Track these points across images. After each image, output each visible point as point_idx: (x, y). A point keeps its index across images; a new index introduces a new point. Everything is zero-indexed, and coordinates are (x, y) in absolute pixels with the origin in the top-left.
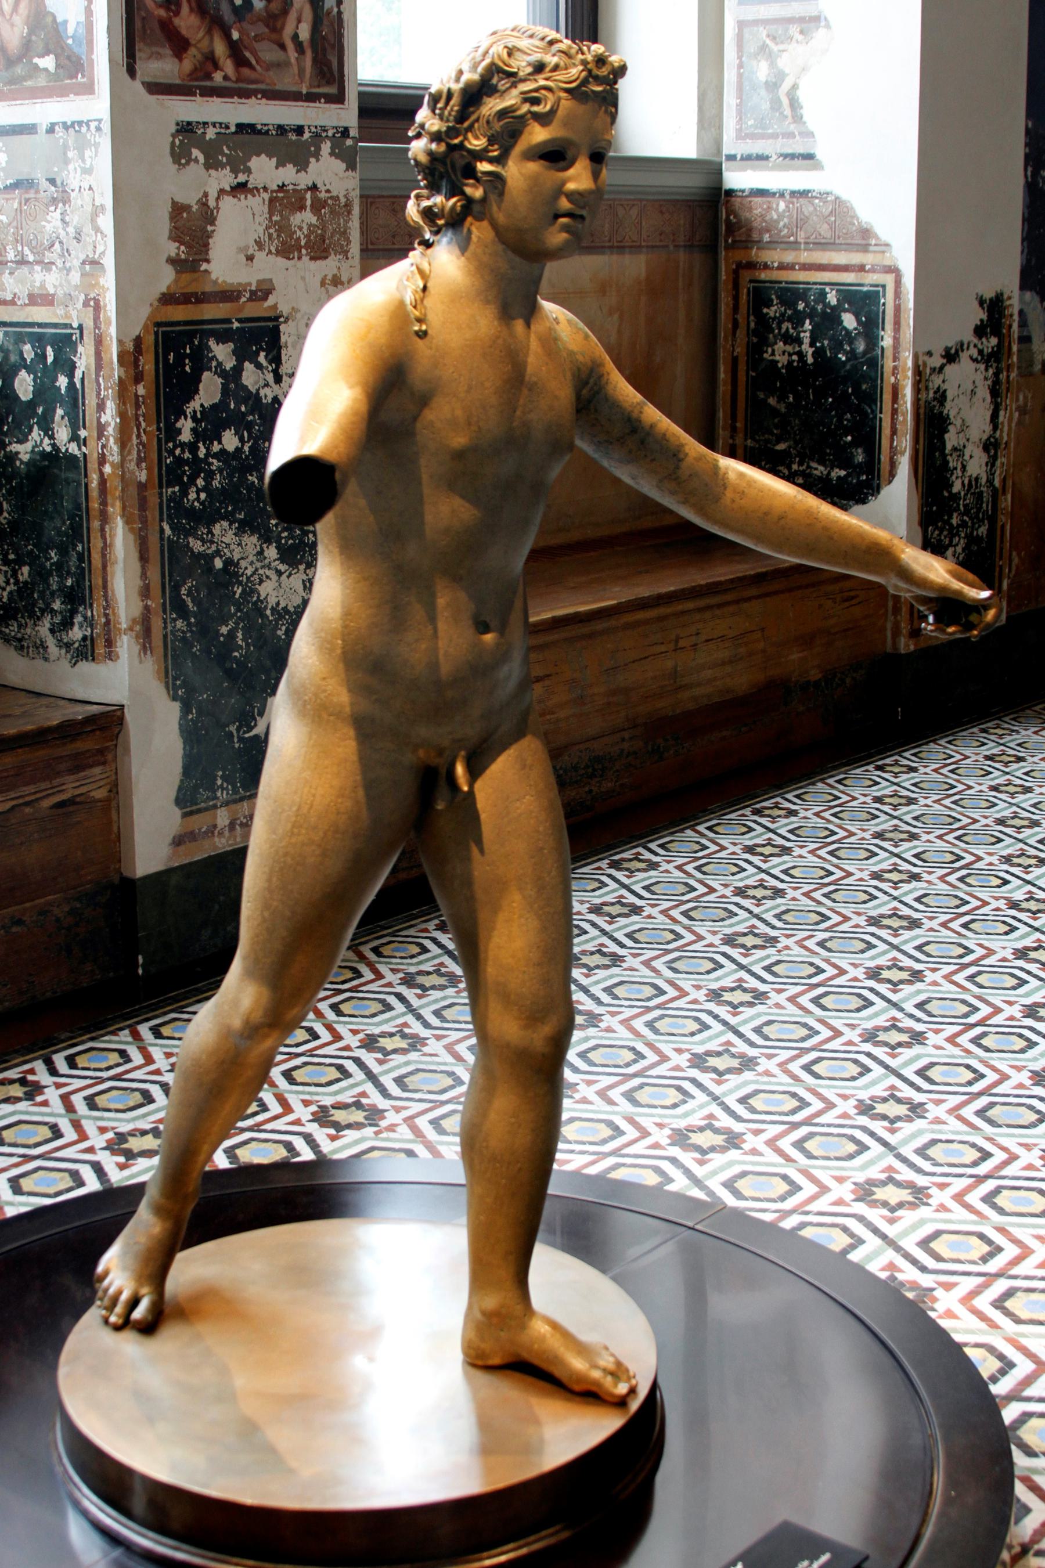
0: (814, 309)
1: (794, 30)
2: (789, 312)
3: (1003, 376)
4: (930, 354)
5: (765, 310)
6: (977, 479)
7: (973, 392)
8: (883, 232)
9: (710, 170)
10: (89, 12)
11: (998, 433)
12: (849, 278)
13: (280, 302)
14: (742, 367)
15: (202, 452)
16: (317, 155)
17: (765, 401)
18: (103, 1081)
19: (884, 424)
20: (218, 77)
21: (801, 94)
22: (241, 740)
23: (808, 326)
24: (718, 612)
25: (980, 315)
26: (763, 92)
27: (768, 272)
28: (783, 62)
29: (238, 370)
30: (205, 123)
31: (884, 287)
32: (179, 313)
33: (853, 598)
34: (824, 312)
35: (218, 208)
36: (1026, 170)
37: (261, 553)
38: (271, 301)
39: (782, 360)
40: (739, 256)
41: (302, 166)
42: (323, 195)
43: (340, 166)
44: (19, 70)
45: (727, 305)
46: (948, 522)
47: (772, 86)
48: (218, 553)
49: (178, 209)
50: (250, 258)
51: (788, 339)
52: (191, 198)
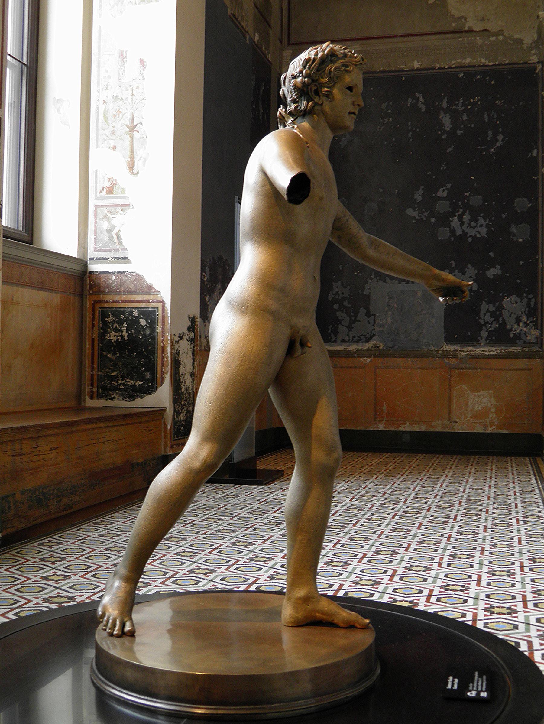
0: (128, 318)
2: (117, 320)
5: (106, 319)
6: (189, 387)
8: (157, 287)
11: (194, 371)
12: (143, 305)
14: (96, 342)
17: (106, 356)
19: (158, 362)
21: (121, 234)
24: (111, 429)
26: (106, 233)
27: (108, 304)
28: (113, 222)
31: (157, 308)
33: (152, 430)
34: (132, 319)
39: (114, 339)
40: (96, 298)
45: (90, 317)
46: (180, 403)
47: (109, 231)
51: (116, 330)
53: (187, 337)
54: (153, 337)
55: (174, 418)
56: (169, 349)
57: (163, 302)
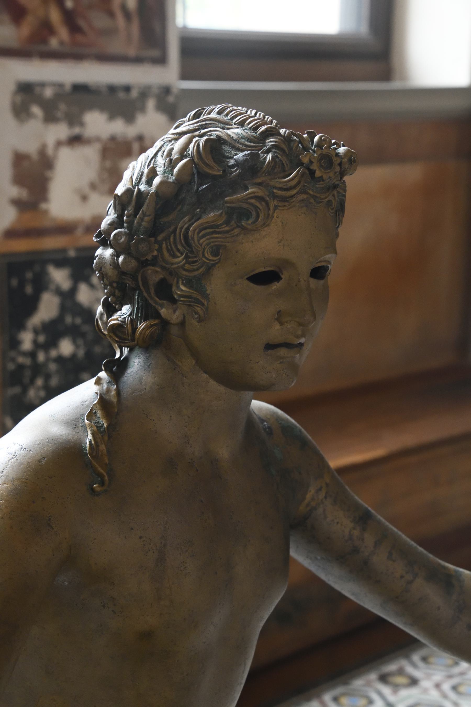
15: (41, 357)
16: (143, 109)
20: (54, 43)
29: (73, 291)
30: (43, 85)
32: (21, 246)
35: (55, 156)
49: (19, 159)
50: (84, 198)
52: (30, 147)
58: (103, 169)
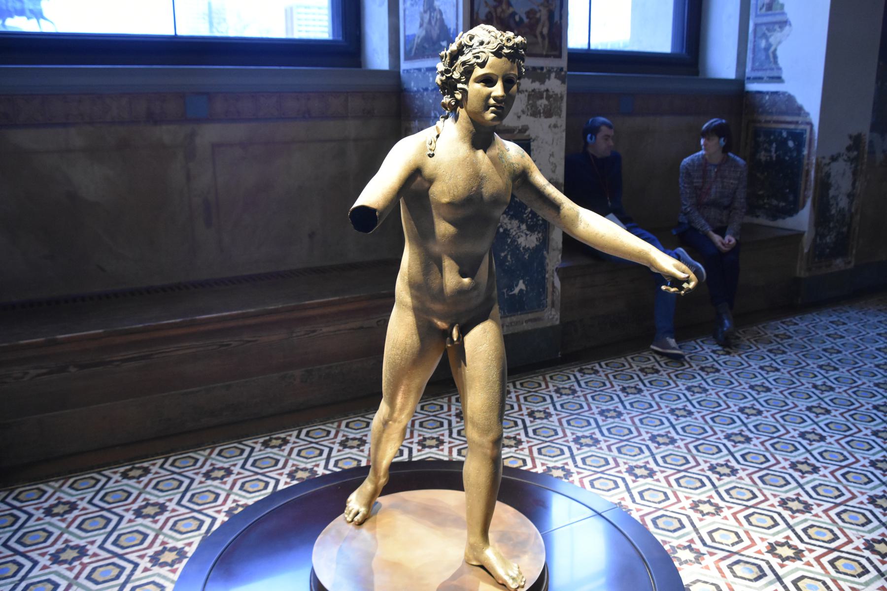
1: (777, 27)
3: (859, 168)
4: (824, 158)
7: (844, 174)
8: (807, 108)
9: (739, 82)
10: (457, 25)
12: (792, 127)
13: (531, 133)
16: (549, 78)
18: (429, 416)
21: (779, 53)
22: (508, 295)
23: (774, 145)
25: (849, 142)
36: (877, 82)
37: (519, 227)
38: (527, 133)
39: (763, 159)
41: (542, 82)
42: (551, 93)
43: (558, 82)
44: (436, 47)
47: (767, 49)
48: (501, 226)
50: (519, 117)
53: (846, 158)
54: (799, 159)
55: (814, 240)
56: (813, 173)
57: (810, 124)
58: (528, 104)
